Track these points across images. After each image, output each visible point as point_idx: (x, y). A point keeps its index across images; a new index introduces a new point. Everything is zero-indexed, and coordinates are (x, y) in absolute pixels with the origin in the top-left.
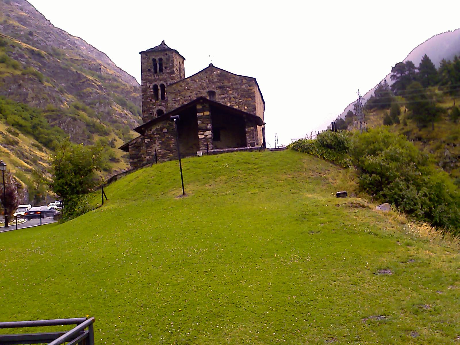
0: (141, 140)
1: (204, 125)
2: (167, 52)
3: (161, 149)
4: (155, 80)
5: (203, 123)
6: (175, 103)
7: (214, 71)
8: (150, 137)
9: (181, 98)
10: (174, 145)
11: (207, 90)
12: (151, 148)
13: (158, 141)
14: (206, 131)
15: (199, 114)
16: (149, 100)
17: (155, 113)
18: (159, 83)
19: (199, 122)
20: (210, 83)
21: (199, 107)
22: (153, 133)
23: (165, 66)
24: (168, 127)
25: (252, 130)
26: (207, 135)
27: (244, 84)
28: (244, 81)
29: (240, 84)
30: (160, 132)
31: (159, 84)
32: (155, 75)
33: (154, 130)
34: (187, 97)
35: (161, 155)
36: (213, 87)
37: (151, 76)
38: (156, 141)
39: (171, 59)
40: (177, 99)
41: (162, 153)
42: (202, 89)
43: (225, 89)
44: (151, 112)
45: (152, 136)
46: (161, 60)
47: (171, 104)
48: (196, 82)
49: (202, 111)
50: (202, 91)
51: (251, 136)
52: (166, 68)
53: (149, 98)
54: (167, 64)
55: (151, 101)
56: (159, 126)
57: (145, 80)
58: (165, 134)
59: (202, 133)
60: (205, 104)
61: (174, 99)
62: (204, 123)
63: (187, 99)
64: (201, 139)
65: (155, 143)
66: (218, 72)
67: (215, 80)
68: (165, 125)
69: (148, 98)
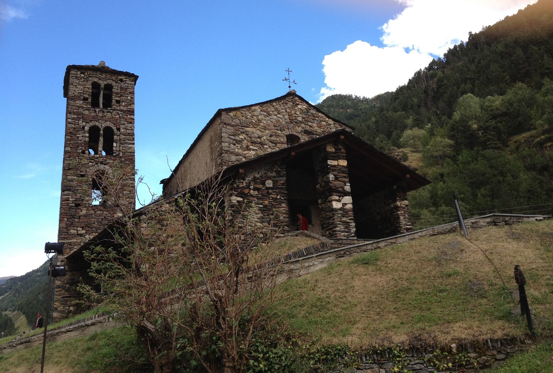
2: (123, 77)
3: (262, 222)
4: (95, 118)
5: (336, 178)
6: (234, 145)
7: (298, 104)
8: (241, 194)
9: (245, 138)
10: (285, 215)
11: (287, 132)
13: (256, 204)
14: (343, 197)
15: (331, 161)
16: (80, 151)
18: (102, 125)
20: (292, 123)
21: (330, 149)
22: (248, 187)
23: (119, 99)
24: (274, 177)
25: (407, 206)
30: (261, 186)
31: (103, 125)
32: (97, 110)
33: (250, 179)
36: (297, 130)
37: (88, 109)
39: (129, 90)
40: (237, 138)
42: (279, 128)
44: (83, 173)
45: (246, 191)
46: (109, 87)
47: (227, 144)
48: (270, 115)
49: (336, 158)
50: (279, 132)
51: (406, 215)
53: (81, 147)
54: (121, 96)
55: (83, 152)
56: (258, 173)
57: (74, 113)
58: (270, 191)
59: (337, 198)
60: (340, 147)
61: (232, 137)
62: (339, 181)
64: (336, 210)
66: (304, 107)
67: (300, 119)
68: (270, 174)
69: (78, 147)
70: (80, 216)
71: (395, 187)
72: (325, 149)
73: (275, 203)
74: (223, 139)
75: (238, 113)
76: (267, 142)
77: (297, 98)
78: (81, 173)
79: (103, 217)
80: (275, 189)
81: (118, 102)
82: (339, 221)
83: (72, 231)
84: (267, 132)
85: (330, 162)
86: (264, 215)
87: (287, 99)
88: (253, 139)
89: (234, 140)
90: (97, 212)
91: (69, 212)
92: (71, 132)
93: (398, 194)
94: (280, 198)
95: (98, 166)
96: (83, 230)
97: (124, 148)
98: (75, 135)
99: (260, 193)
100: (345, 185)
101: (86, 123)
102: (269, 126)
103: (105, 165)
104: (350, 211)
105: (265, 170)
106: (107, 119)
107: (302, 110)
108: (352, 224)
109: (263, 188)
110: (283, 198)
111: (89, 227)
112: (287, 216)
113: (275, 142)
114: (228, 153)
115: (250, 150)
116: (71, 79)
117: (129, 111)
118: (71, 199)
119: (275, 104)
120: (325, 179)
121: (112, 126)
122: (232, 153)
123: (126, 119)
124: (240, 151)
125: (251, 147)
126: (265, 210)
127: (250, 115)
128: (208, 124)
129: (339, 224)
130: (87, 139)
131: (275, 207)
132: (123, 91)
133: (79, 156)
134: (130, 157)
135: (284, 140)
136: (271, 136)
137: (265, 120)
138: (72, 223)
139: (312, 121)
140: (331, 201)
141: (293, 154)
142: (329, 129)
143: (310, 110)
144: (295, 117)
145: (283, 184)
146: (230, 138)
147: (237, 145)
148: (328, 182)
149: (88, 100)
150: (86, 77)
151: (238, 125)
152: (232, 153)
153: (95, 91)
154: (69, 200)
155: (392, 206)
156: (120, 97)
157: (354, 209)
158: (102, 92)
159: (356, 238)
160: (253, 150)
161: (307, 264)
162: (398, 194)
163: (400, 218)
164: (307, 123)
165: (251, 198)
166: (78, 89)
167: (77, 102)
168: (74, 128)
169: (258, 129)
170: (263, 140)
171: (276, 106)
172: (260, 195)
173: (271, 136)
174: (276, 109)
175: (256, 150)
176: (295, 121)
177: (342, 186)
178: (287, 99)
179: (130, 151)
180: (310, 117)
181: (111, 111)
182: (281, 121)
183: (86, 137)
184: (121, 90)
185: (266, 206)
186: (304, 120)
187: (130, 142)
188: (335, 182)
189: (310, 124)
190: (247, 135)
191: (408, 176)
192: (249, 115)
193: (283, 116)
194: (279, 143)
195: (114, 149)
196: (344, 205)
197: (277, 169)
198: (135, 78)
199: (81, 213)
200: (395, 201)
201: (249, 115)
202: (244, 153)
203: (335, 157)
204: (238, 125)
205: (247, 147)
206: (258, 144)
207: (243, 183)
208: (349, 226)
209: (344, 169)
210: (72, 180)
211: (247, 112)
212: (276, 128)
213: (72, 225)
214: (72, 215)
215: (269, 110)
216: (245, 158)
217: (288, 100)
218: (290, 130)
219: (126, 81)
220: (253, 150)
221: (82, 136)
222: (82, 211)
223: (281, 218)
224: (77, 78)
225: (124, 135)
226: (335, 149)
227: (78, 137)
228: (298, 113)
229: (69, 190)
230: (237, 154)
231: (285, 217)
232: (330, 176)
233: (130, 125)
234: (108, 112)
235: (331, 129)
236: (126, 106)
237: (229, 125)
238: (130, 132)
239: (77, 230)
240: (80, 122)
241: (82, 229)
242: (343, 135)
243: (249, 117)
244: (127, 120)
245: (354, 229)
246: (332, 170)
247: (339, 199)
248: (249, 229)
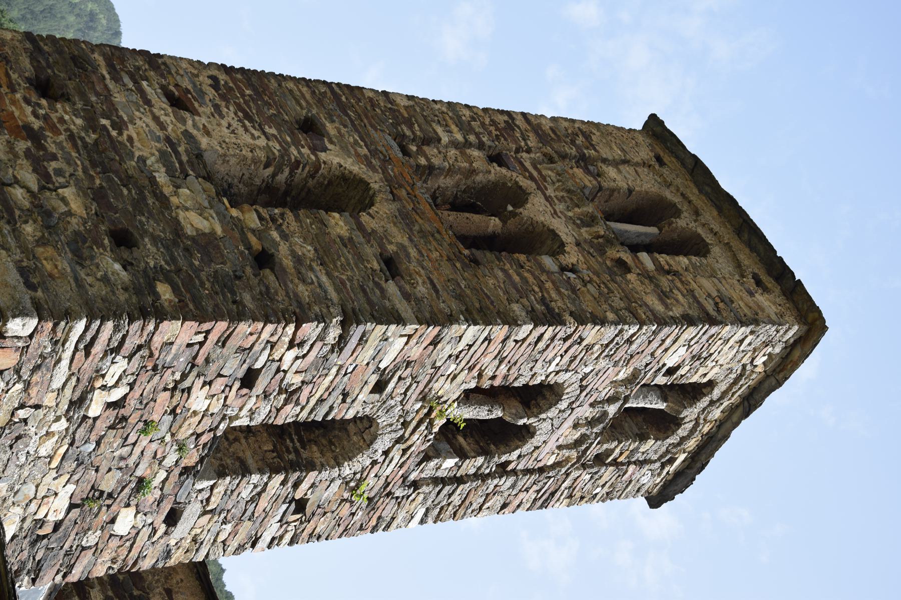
78: (395, 379)
111: (112, 427)
239: (116, 385)
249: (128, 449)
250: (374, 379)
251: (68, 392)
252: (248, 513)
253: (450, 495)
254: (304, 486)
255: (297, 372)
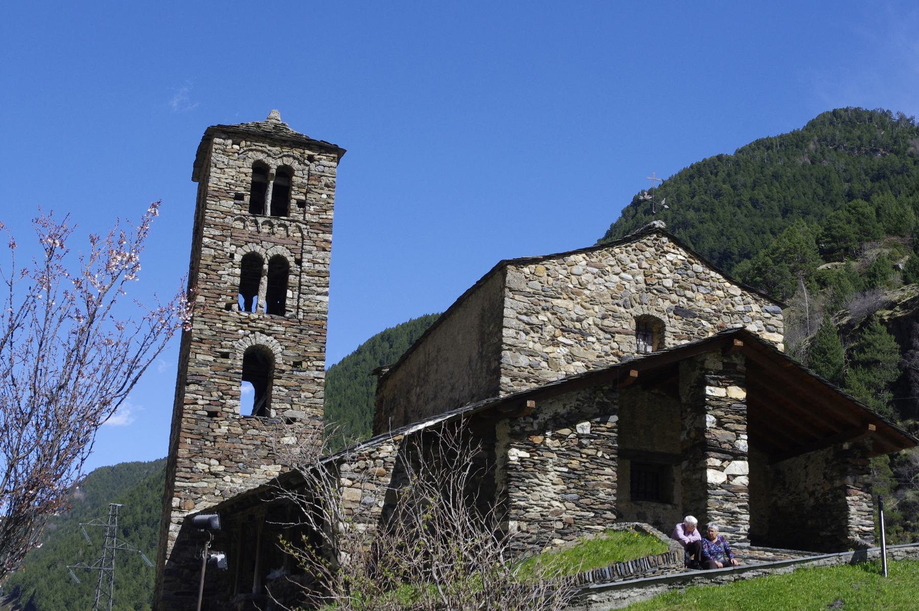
0: (390, 448)
1: (730, 436)
4: (255, 238)
5: (720, 424)
6: (527, 334)
10: (610, 490)
11: (638, 311)
12: (530, 488)
14: (730, 461)
15: (712, 388)
16: (223, 305)
17: (240, 356)
18: (267, 252)
19: (710, 420)
20: (649, 290)
21: (713, 362)
23: (303, 198)
26: (735, 476)
27: (753, 319)
28: (755, 307)
29: (742, 314)
31: (270, 253)
32: (261, 220)
33: (547, 417)
34: (572, 320)
35: (559, 525)
36: (660, 308)
38: (549, 467)
39: (324, 180)
40: (533, 320)
41: (564, 516)
43: (695, 320)
44: (225, 350)
46: (285, 173)
47: (511, 332)
48: (604, 273)
50: (622, 309)
51: (865, 504)
52: (301, 204)
56: (564, 406)
58: (585, 442)
59: (718, 463)
60: (735, 360)
61: (524, 318)
62: (726, 429)
63: (571, 326)
64: (714, 487)
65: (546, 472)
67: (668, 283)
70: (215, 437)
71: (846, 446)
72: (703, 362)
73: (591, 466)
74: (506, 322)
75: (540, 268)
76: (594, 329)
77: (665, 239)
78: (222, 350)
79: (259, 443)
80: (595, 438)
81: (301, 204)
82: (717, 509)
83: (200, 466)
84: (597, 308)
85: (709, 390)
86: (569, 488)
87: (645, 241)
88: (566, 323)
89: (528, 324)
90: (248, 432)
91: (196, 427)
92: (208, 265)
93: (849, 459)
94: (603, 457)
95: (255, 338)
96: (220, 464)
97: (307, 303)
98: (214, 270)
99: (565, 444)
100: (738, 436)
101: (237, 246)
102: (601, 296)
103: (269, 335)
104: (741, 490)
105: (577, 400)
106: (277, 240)
107: (675, 264)
108: (742, 517)
109: (571, 436)
110: (608, 457)
111: (231, 460)
112: (614, 491)
113: (610, 329)
114: (514, 349)
115: (557, 344)
116: (214, 154)
117: (321, 224)
118: (200, 402)
119: (617, 250)
120: (697, 425)
121: (286, 254)
122: (521, 350)
123: (315, 241)
124: (538, 347)
125: (561, 339)
126: (570, 478)
127: (565, 272)
128: (478, 282)
129: (716, 515)
130: (237, 281)
131: (590, 474)
132: (313, 182)
133: (220, 315)
134: (318, 322)
135: (631, 326)
136: (603, 318)
137: (594, 284)
138: (201, 451)
139: (695, 288)
140: (705, 468)
141: (634, 373)
142: (730, 306)
143: (692, 264)
144: (660, 279)
145: (610, 430)
146: (520, 320)
147: (532, 334)
148: (702, 429)
149: (243, 199)
150: (242, 150)
151: (538, 294)
152: (521, 350)
153: (258, 179)
154: (196, 404)
155: (837, 483)
156: (305, 194)
157: (752, 487)
158: (272, 182)
159: (748, 544)
160: (565, 345)
161: (617, 595)
162: (849, 459)
163: (848, 509)
164: (682, 294)
165: (547, 454)
166: (226, 176)
167: (223, 202)
168: (215, 257)
169: (578, 303)
170: (586, 326)
171: (621, 255)
172: (563, 449)
173: (603, 318)
174: (619, 261)
175: (571, 345)
176: (657, 287)
177: (732, 439)
178: (645, 241)
179: (318, 308)
180: (690, 279)
181: (287, 223)
182: (627, 286)
183: (234, 276)
184: (308, 180)
185: (575, 469)
186: (677, 285)
187: (320, 290)
188: (717, 431)
189: (689, 294)
190: (553, 314)
191: (872, 427)
192: (562, 273)
193: (633, 276)
194: (619, 333)
195: (288, 302)
196: (731, 478)
197: (602, 398)
198: (336, 152)
199: (218, 432)
200: (843, 474)
201: (562, 273)
202: (545, 351)
203: (721, 380)
204: (538, 294)
205: (554, 338)
206: (575, 333)
207: (532, 424)
208: (737, 519)
209: (739, 405)
210: (205, 364)
211: (558, 267)
212: (616, 301)
213: (201, 452)
214: (200, 434)
215: (604, 263)
216: (547, 360)
217: (645, 244)
218: (644, 306)
219: (321, 159)
220: (565, 345)
221: (228, 275)
222: (220, 427)
223: (602, 495)
224: (224, 152)
225: (308, 274)
226: (724, 363)
227: (221, 276)
228: (665, 270)
229: (198, 383)
230: (532, 354)
231: (610, 495)
232: (708, 419)
233: (322, 254)
234: (280, 226)
235: (733, 306)
236: (317, 213)
237: (520, 292)
238: (322, 268)
239: (210, 465)
240: (227, 244)
241: (217, 463)
242: (739, 339)
243: (561, 276)
244: (318, 244)
245: (747, 527)
246: (713, 406)
247: (722, 466)
248: (534, 513)
249: (244, 451)
250: (219, 360)
251: (209, 480)
252: (296, 388)
253: (308, 286)
254: (284, 367)
255: (211, 396)
